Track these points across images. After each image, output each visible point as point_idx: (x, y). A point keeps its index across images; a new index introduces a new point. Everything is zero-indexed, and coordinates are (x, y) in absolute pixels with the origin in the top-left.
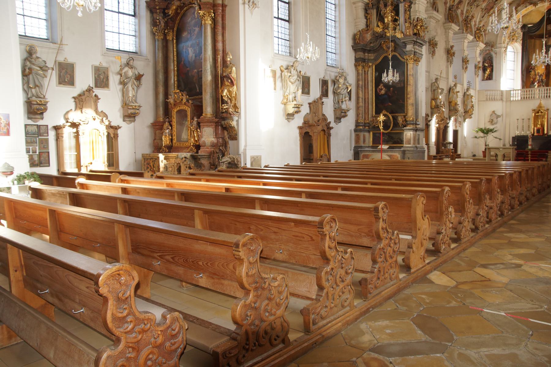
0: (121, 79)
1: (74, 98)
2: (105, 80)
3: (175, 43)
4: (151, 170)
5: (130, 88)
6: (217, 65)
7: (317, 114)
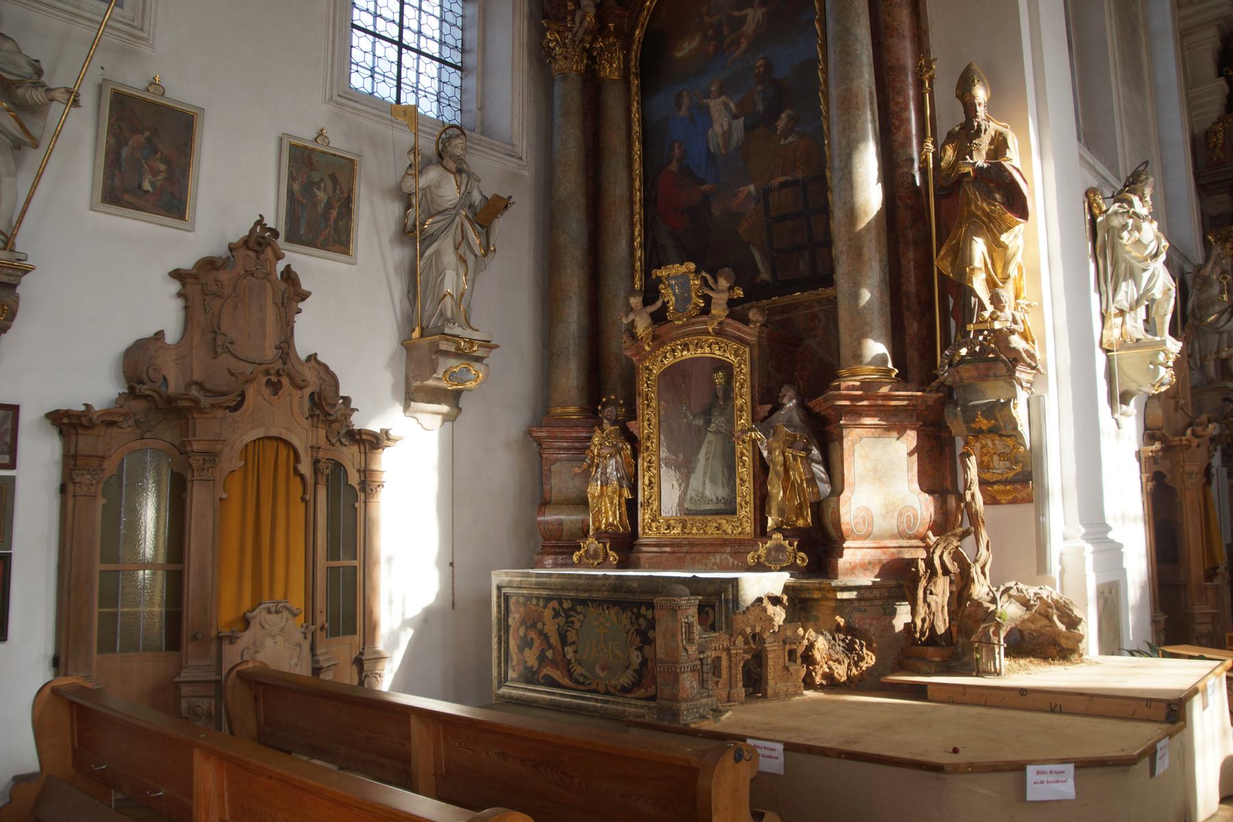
0: (406, 216)
1: (177, 274)
2: (334, 213)
3: (634, 89)
4: (549, 654)
5: (450, 258)
6: (900, 137)
7: (1182, 402)
